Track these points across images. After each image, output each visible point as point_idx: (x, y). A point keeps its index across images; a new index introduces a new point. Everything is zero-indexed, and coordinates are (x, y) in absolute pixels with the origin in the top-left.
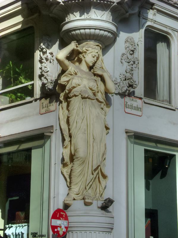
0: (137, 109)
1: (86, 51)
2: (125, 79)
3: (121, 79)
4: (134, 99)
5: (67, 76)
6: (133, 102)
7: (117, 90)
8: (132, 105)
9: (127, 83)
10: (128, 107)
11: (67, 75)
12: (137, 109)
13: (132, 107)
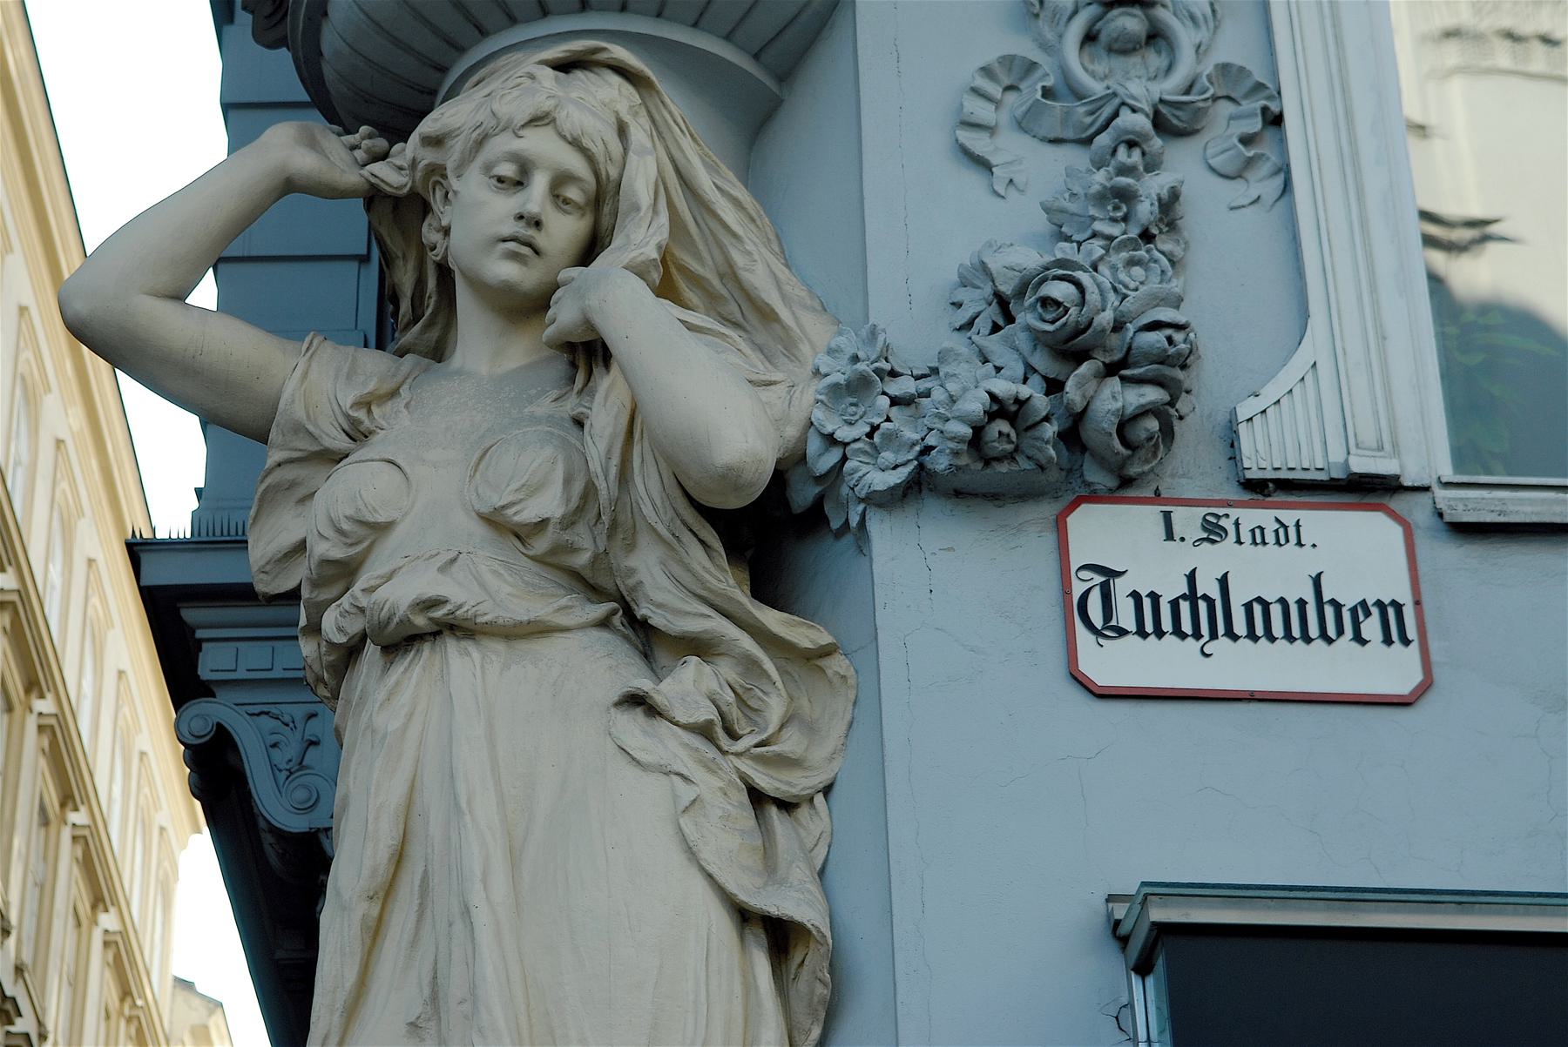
0: (1317, 618)
4: (1252, 517)
5: (293, 485)
6: (1210, 563)
7: (888, 457)
10: (1129, 622)
12: (1317, 618)
13: (1203, 614)
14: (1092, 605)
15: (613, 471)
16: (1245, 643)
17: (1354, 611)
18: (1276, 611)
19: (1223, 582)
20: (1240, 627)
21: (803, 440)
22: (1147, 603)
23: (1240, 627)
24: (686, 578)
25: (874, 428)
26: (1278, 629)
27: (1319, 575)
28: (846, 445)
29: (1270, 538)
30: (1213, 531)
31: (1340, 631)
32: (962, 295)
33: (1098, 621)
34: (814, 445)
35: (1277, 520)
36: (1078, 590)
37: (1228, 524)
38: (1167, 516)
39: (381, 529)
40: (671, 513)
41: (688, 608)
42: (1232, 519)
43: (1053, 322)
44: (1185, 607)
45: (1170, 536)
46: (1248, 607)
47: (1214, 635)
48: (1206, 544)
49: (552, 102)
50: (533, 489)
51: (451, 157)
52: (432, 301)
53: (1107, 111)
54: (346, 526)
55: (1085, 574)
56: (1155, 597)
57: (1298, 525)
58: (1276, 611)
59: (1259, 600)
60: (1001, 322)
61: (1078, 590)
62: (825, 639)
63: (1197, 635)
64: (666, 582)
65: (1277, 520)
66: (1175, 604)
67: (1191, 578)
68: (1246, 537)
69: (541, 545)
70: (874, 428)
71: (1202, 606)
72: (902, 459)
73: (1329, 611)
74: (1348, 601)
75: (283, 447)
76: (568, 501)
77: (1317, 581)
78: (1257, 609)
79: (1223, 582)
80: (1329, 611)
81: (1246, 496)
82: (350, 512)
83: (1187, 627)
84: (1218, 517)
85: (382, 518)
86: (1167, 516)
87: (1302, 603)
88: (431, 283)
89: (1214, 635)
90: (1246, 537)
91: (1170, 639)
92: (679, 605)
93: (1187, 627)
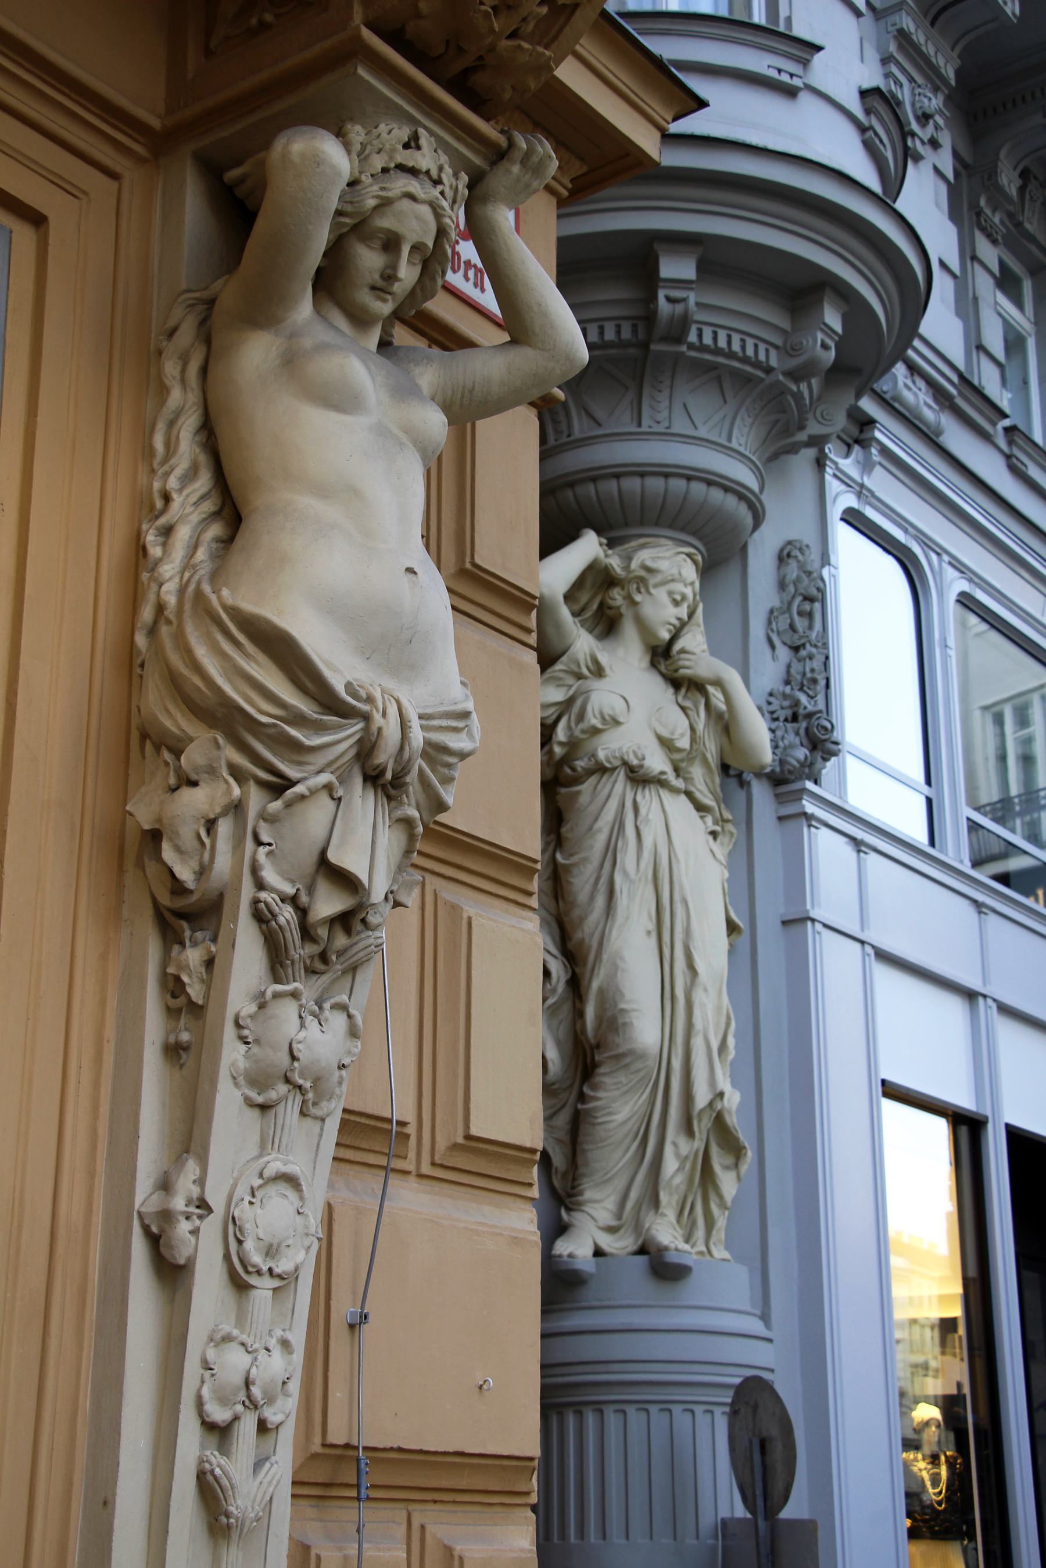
2: (795, 718)
3: (775, 716)
5: (560, 679)
9: (802, 732)
11: (561, 675)
32: (772, 699)
39: (616, 723)
53: (802, 641)
54: (607, 718)
62: (730, 817)
64: (702, 781)
69: (677, 756)
75: (565, 665)
82: (611, 713)
88: (595, 606)
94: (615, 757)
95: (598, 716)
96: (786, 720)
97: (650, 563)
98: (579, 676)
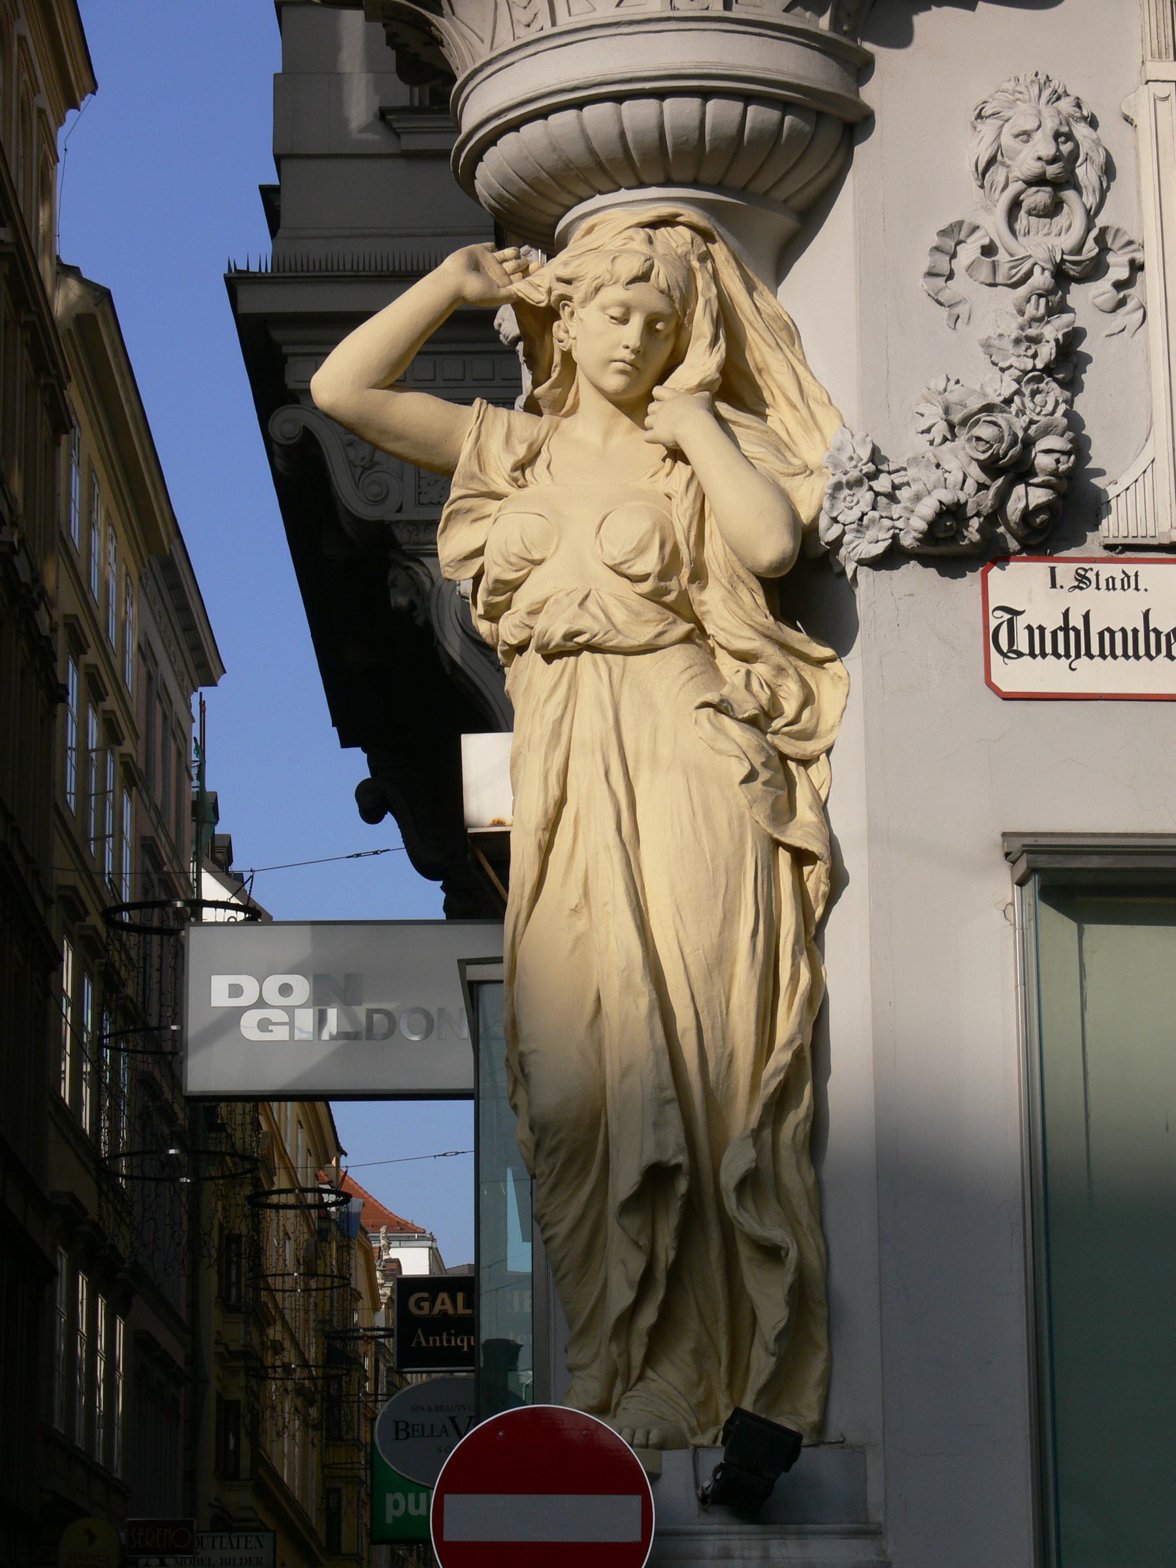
1: (561, 289)
5: (469, 511)
6: (1079, 603)
7: (871, 534)
8: (1076, 621)
14: (1001, 636)
15: (692, 539)
16: (1098, 660)
17: (1168, 636)
18: (1119, 637)
19: (1086, 617)
20: (1095, 650)
21: (816, 520)
22: (1037, 633)
23: (1095, 650)
24: (740, 613)
25: (864, 514)
26: (1119, 651)
27: (1148, 611)
28: (845, 525)
29: (1118, 585)
30: (1082, 580)
31: (1158, 651)
33: (1005, 648)
34: (823, 522)
35: (1124, 572)
36: (993, 624)
37: (1091, 575)
38: (1053, 570)
40: (730, 571)
41: (742, 634)
42: (1094, 572)
43: (984, 452)
44: (1061, 635)
45: (1054, 585)
46: (1101, 635)
47: (1078, 656)
48: (1077, 590)
49: (648, 263)
50: (640, 550)
51: (578, 292)
52: (558, 369)
53: (1026, 267)
54: (513, 559)
55: (999, 613)
56: (1042, 629)
57: (1136, 575)
58: (1119, 637)
59: (1109, 630)
60: (949, 437)
61: (993, 624)
63: (1067, 655)
64: (725, 613)
65: (1124, 572)
66: (1054, 634)
67: (1066, 615)
68: (1103, 584)
70: (864, 514)
71: (1072, 634)
72: (882, 536)
73: (1152, 635)
74: (1165, 629)
75: (462, 487)
76: (663, 559)
77: (1146, 615)
78: (1107, 635)
79: (1086, 617)
80: (1152, 635)
81: (1105, 554)
83: (1061, 651)
84: (1086, 571)
85: (537, 556)
86: (1053, 570)
87: (1135, 631)
89: (1078, 656)
90: (1103, 584)
91: (1051, 659)
92: (735, 631)
93: (1061, 651)
94: (516, 626)
95: (501, 561)
96: (945, 439)
97: (566, 273)
98: (498, 497)
